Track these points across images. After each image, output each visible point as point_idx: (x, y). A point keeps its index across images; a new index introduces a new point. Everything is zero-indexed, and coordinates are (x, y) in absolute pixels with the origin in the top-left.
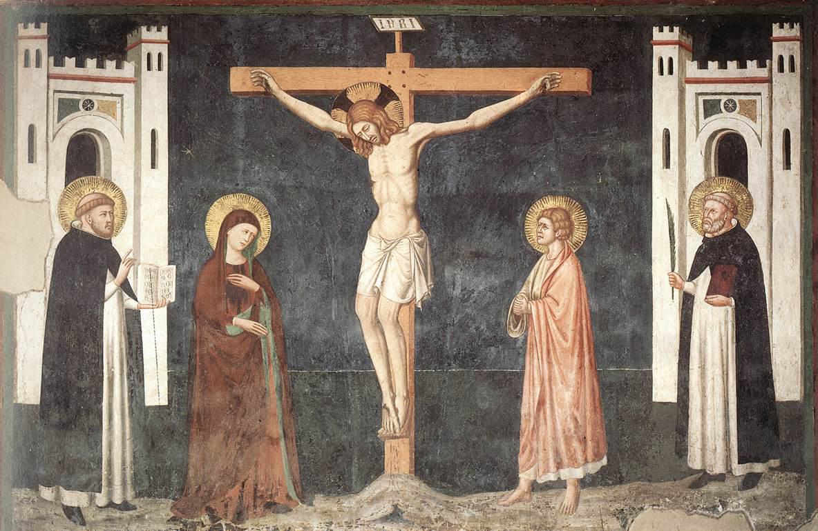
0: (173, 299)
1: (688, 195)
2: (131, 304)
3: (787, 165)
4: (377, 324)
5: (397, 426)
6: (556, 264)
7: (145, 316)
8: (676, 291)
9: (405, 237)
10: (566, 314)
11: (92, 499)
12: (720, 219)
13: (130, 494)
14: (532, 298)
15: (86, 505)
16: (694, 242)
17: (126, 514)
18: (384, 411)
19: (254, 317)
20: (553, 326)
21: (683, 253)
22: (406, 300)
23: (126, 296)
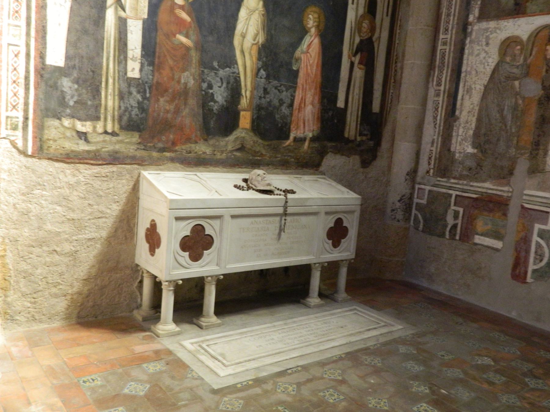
0: (146, 16)
1: (358, 18)
2: (122, 14)
3: (387, 15)
4: (243, 52)
5: (246, 105)
6: (313, 38)
7: (130, 22)
8: (349, 60)
9: (257, 9)
10: (313, 62)
11: (95, 127)
12: (366, 32)
13: (117, 127)
14: (303, 53)
15: (91, 132)
16: (357, 40)
17: (114, 139)
18: (242, 97)
19: (187, 36)
20: (309, 67)
21: (353, 43)
22: (256, 42)
23: (119, 9)
